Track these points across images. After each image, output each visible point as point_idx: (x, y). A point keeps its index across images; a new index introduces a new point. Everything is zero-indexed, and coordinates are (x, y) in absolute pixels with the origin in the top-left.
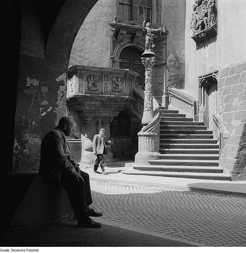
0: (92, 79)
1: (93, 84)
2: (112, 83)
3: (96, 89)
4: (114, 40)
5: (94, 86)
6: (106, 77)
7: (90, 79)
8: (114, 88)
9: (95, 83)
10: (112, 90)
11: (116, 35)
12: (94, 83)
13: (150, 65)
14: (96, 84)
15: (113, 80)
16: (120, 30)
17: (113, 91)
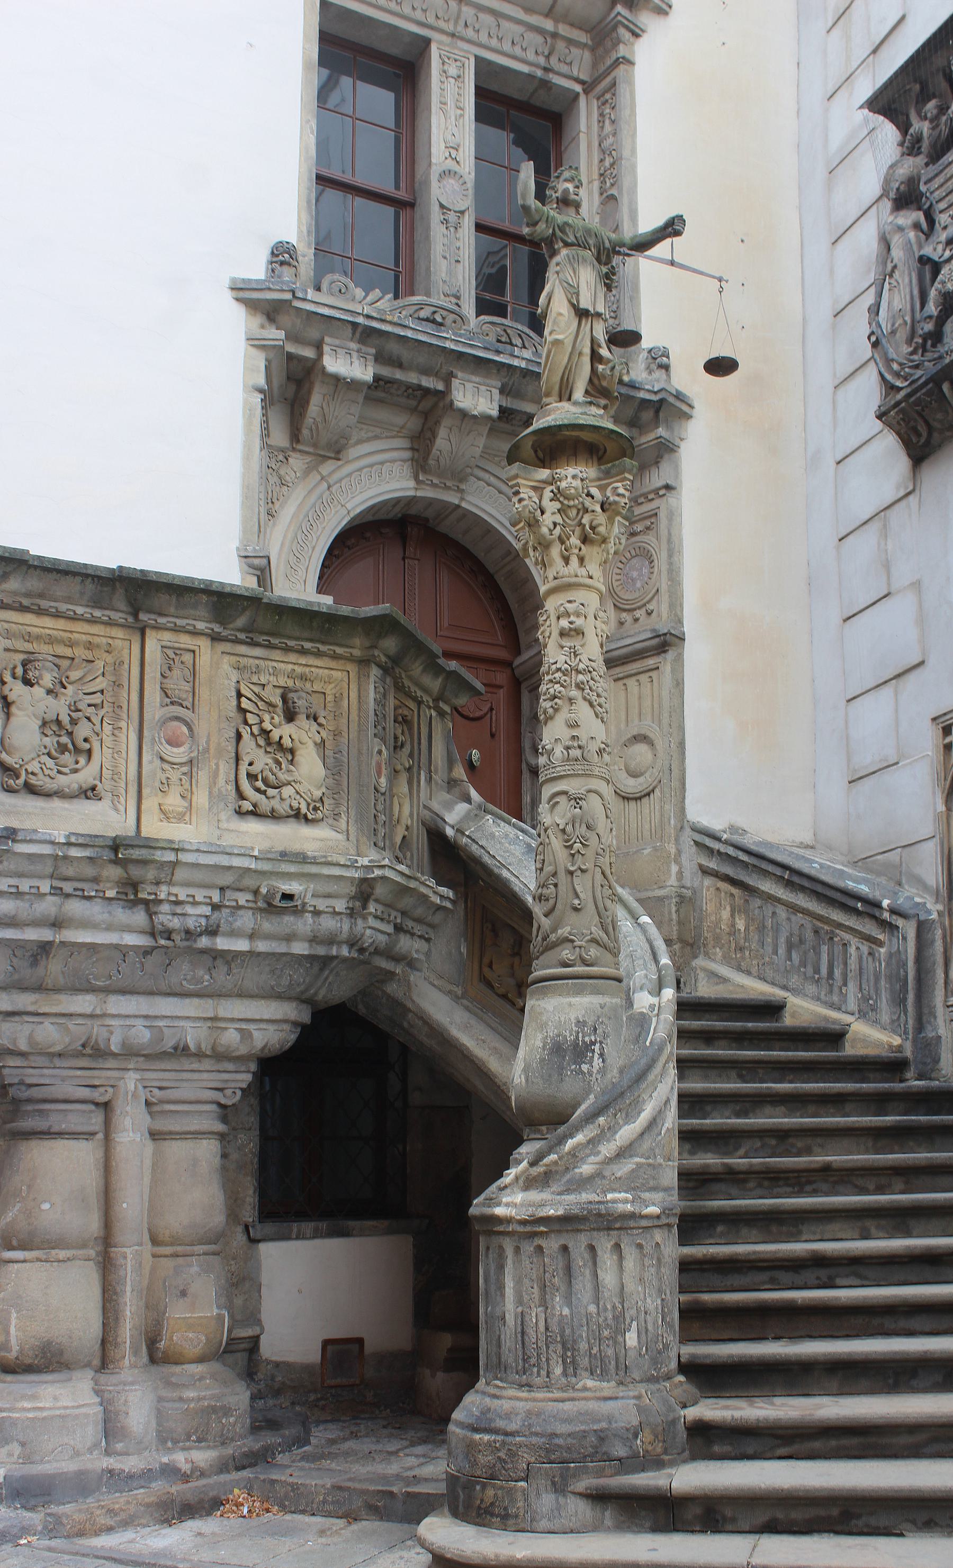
0: (48, 679)
1: (50, 724)
2: (239, 736)
3: (87, 776)
4: (280, 438)
5: (63, 749)
6: (176, 672)
7: (27, 682)
8: (252, 777)
9: (74, 722)
10: (241, 796)
11: (291, 389)
12: (65, 720)
13: (585, 540)
14: (83, 730)
15: (245, 704)
16: (326, 349)
17: (247, 806)
